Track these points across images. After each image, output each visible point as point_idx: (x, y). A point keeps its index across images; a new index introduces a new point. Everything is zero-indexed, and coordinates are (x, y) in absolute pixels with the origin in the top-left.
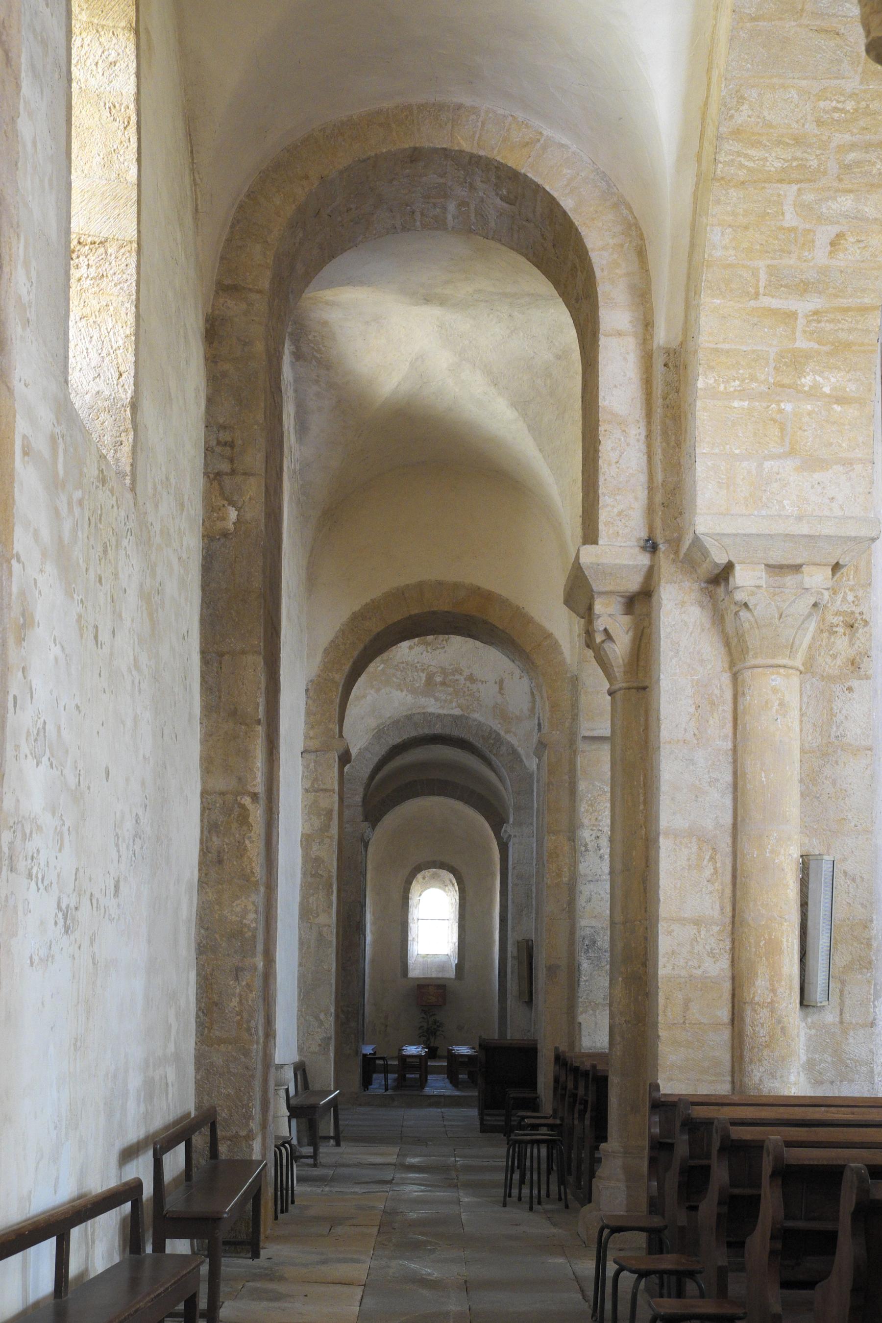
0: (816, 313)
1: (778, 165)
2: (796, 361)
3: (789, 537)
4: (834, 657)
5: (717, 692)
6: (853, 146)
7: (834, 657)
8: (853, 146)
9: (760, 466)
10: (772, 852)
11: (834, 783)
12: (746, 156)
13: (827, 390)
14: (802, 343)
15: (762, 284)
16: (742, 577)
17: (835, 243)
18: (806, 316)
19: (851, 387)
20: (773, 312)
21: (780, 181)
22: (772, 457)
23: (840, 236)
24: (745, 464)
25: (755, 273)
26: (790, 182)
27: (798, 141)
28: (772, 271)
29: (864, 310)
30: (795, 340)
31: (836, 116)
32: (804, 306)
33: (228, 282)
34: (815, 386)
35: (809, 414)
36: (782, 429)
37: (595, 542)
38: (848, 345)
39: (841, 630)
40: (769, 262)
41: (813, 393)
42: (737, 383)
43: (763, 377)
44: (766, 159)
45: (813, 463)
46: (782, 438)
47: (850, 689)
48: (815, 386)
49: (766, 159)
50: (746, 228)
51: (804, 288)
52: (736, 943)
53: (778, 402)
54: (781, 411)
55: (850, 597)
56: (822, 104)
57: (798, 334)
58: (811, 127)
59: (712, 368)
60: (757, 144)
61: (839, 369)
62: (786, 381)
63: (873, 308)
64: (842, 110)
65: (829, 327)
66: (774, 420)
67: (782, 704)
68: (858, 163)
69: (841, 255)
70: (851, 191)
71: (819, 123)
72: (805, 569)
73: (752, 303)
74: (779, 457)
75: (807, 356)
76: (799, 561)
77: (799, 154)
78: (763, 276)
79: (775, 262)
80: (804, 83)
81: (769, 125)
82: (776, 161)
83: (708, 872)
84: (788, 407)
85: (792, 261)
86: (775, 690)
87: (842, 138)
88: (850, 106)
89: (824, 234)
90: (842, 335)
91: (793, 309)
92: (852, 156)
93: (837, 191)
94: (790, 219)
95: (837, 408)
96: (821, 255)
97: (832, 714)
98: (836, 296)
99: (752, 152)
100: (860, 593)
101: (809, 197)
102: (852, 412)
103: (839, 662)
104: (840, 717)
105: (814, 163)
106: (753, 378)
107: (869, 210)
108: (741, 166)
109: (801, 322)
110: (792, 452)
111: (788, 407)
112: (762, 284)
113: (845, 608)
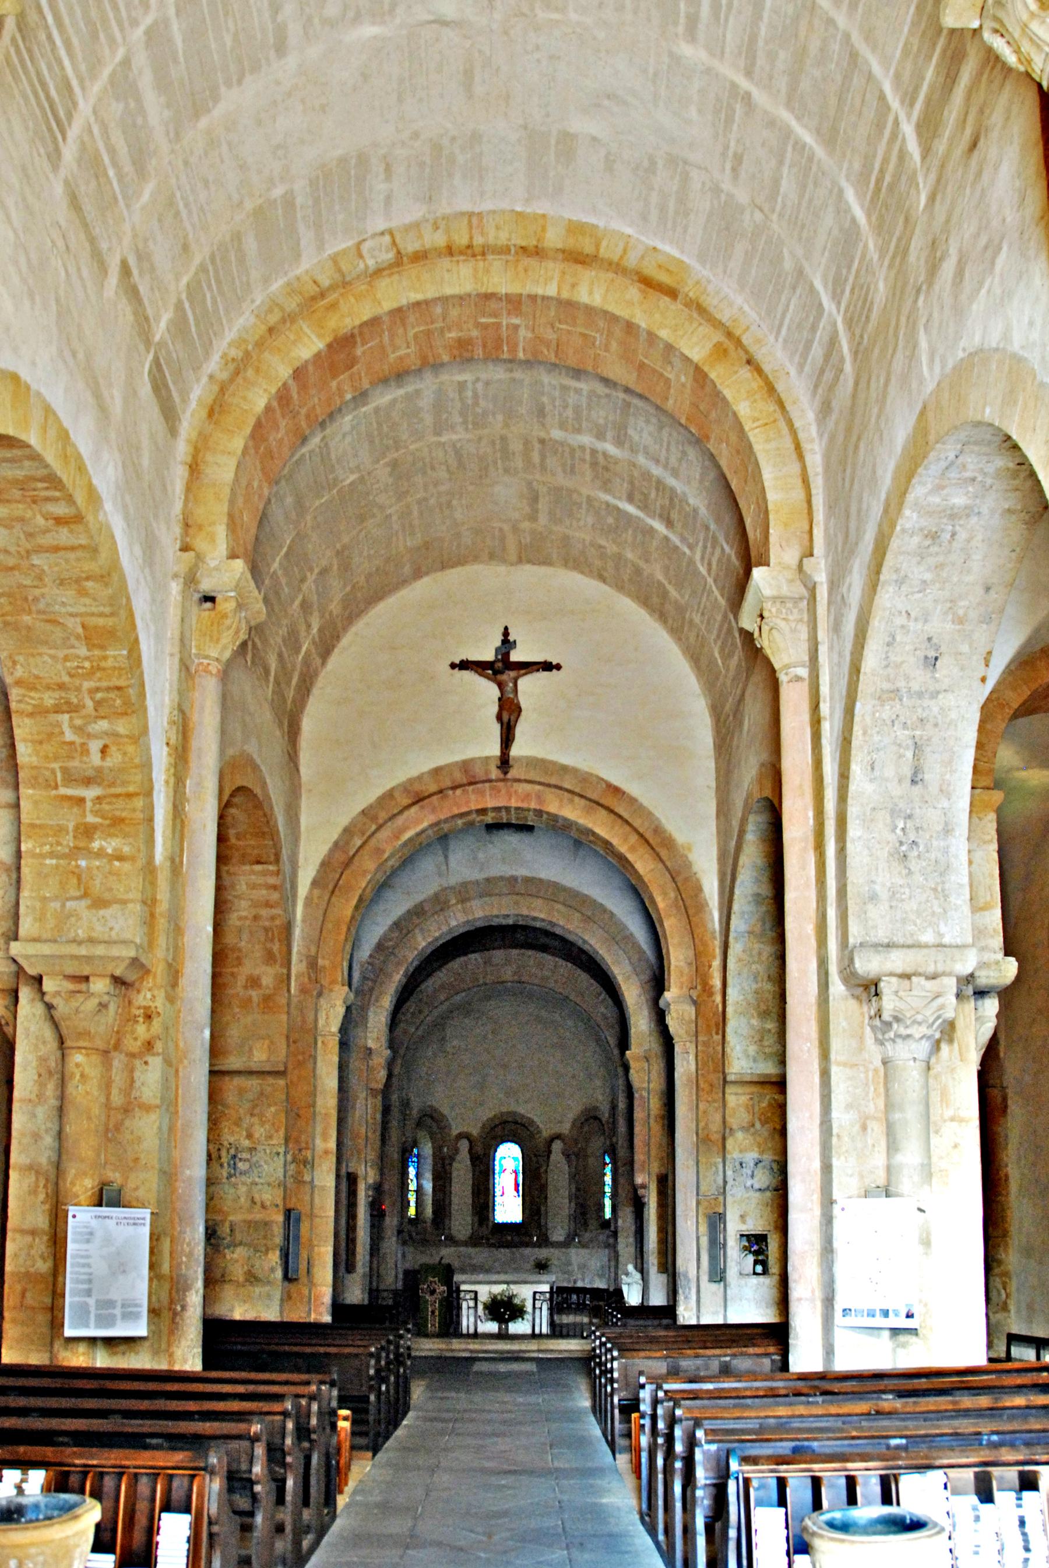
0: (98, 798)
1: (52, 702)
2: (87, 832)
4: (136, 1039)
7: (136, 1039)
9: (63, 906)
13: (109, 851)
16: (48, 985)
17: (104, 751)
19: (126, 849)
20: (69, 798)
21: (56, 712)
24: (52, 904)
25: (53, 772)
26: (63, 712)
27: (61, 686)
28: (65, 770)
29: (129, 796)
30: (85, 816)
32: (90, 793)
34: (102, 849)
36: (79, 879)
38: (122, 820)
39: (141, 1020)
41: (100, 854)
44: (42, 699)
45: (99, 903)
48: (102, 849)
51: (88, 782)
57: (88, 813)
58: (66, 679)
59: (30, 837)
60: (34, 688)
63: (137, 794)
65: (107, 807)
69: (108, 759)
70: (103, 718)
71: (71, 676)
72: (91, 979)
73: (54, 792)
74: (77, 898)
76: (86, 973)
81: (37, 677)
82: (49, 699)
85: (76, 763)
86: (77, 1065)
89: (95, 746)
90: (118, 813)
92: (99, 696)
95: (117, 863)
96: (96, 759)
98: (109, 786)
99: (32, 694)
101: (78, 722)
102: (127, 866)
105: (75, 701)
106: (58, 843)
107: (121, 730)
110: (85, 895)
113: (144, 1003)
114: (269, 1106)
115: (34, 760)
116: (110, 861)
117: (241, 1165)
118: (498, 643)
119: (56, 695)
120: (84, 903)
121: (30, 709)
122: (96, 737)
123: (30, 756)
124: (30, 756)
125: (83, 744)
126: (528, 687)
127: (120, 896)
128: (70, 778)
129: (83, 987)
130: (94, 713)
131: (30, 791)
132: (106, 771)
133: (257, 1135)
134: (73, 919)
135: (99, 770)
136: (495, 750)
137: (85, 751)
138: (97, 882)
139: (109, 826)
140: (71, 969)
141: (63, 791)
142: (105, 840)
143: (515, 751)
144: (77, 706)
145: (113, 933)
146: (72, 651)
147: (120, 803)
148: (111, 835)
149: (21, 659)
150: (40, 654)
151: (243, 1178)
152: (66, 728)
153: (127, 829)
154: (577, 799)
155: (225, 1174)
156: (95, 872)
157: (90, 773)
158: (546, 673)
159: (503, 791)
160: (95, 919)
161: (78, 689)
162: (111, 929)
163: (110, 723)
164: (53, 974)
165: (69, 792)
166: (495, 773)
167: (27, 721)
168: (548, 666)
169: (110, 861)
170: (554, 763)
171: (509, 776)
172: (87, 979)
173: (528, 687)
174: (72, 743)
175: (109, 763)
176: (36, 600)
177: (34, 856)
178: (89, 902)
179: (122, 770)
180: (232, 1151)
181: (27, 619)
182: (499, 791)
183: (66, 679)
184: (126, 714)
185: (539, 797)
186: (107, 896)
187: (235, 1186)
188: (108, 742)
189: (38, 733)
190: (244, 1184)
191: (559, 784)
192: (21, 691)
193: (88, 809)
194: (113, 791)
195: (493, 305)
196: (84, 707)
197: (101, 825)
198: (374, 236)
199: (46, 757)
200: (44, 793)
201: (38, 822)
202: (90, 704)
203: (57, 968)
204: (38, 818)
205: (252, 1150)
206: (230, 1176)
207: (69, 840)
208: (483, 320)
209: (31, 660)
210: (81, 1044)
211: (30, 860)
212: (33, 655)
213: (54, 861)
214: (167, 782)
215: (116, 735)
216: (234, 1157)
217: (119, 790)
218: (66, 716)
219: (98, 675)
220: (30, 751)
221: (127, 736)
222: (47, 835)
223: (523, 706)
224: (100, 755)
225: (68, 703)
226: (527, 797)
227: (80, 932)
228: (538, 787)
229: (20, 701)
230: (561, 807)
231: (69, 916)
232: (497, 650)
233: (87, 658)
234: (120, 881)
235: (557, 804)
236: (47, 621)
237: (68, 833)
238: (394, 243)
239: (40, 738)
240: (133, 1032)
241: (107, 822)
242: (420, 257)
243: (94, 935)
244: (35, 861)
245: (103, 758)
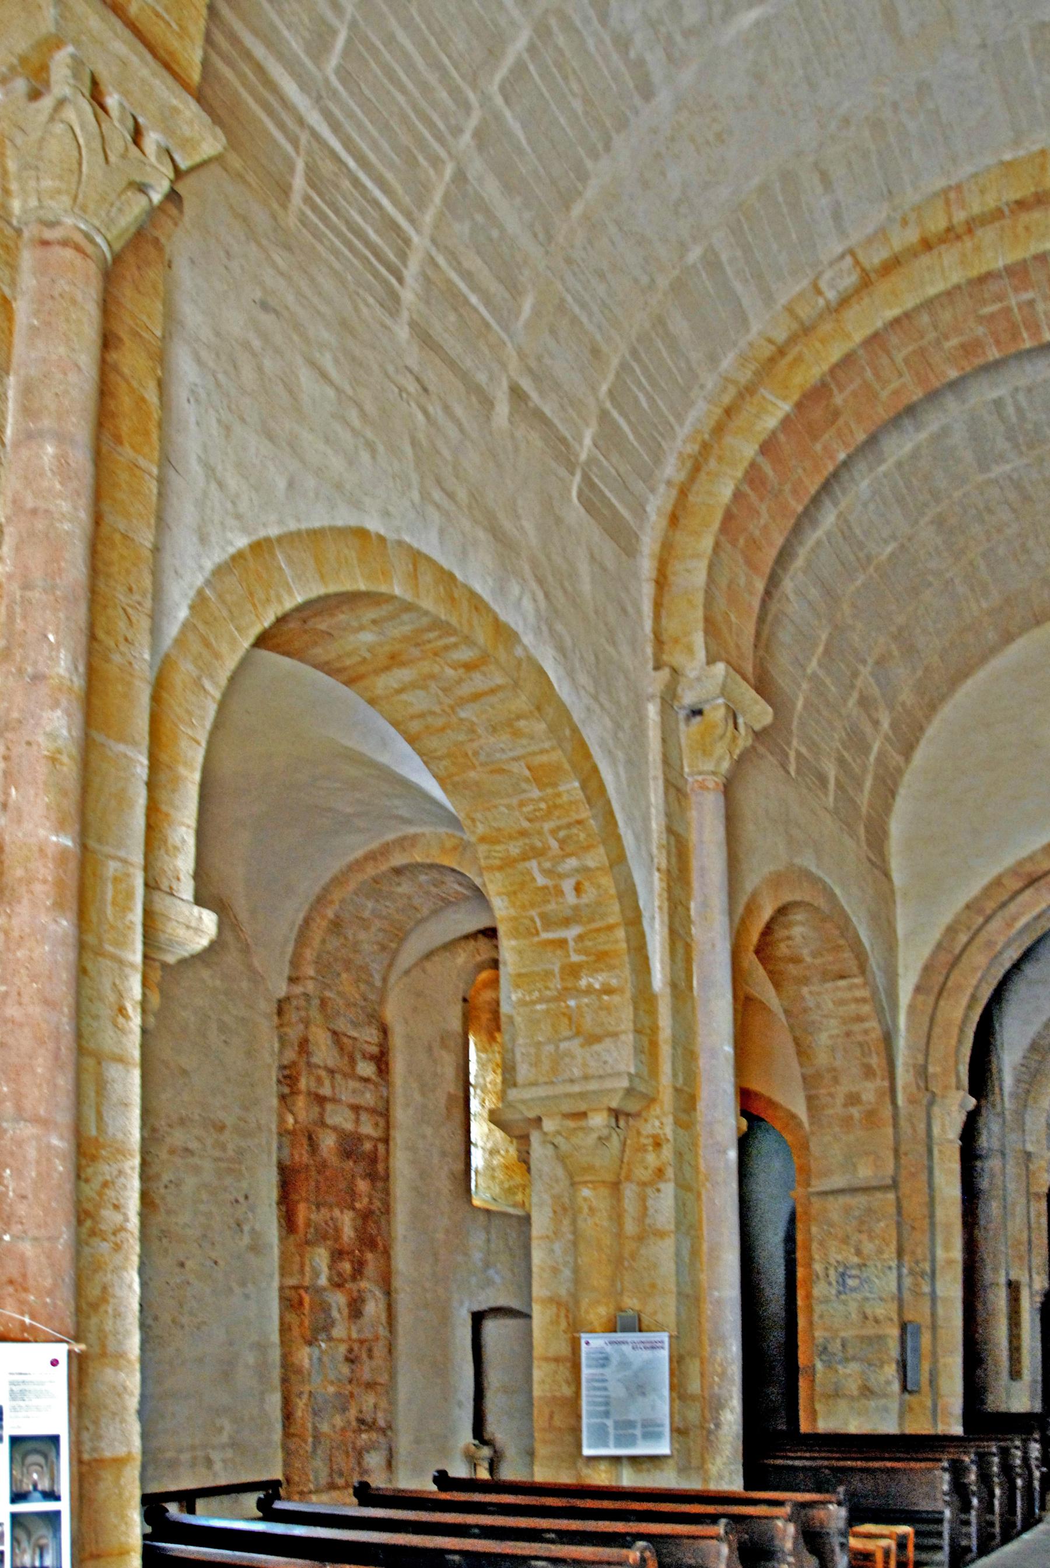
3: (568, 1095)
8: (559, 828)
13: (597, 986)
14: (575, 958)
17: (578, 889)
19: (614, 982)
27: (523, 833)
29: (610, 928)
34: (590, 986)
38: (606, 953)
40: (539, 910)
41: (589, 991)
45: (593, 1039)
46: (570, 1026)
48: (590, 986)
56: (525, 809)
58: (526, 824)
61: (602, 970)
62: (569, 985)
64: (540, 809)
65: (590, 944)
68: (569, 837)
71: (530, 820)
72: (590, 1114)
81: (499, 830)
82: (514, 849)
87: (547, 826)
88: (543, 805)
89: (568, 886)
90: (601, 948)
94: (541, 881)
95: (606, 998)
96: (571, 898)
101: (547, 865)
102: (616, 999)
105: (539, 844)
109: (571, 943)
114: (879, 1220)
116: (599, 999)
117: (850, 1282)
119: (520, 843)
120: (577, 1042)
122: (567, 876)
129: (583, 1123)
133: (865, 1251)
135: (576, 908)
137: (559, 892)
140: (567, 1107)
146: (524, 796)
147: (602, 938)
148: (596, 971)
151: (854, 1295)
155: (834, 1292)
157: (569, 913)
161: (540, 833)
175: (585, 899)
176: (476, 754)
179: (599, 904)
180: (841, 1270)
181: (472, 774)
183: (526, 824)
186: (598, 1031)
187: (845, 1303)
188: (579, 877)
190: (854, 1300)
195: (993, 287)
196: (549, 848)
198: (831, 264)
202: (554, 844)
205: (862, 1266)
206: (839, 1293)
208: (987, 310)
210: (588, 1178)
212: (489, 809)
214: (660, 908)
216: (843, 1275)
224: (574, 893)
225: (533, 848)
233: (542, 799)
236: (492, 772)
238: (857, 262)
242: (891, 265)
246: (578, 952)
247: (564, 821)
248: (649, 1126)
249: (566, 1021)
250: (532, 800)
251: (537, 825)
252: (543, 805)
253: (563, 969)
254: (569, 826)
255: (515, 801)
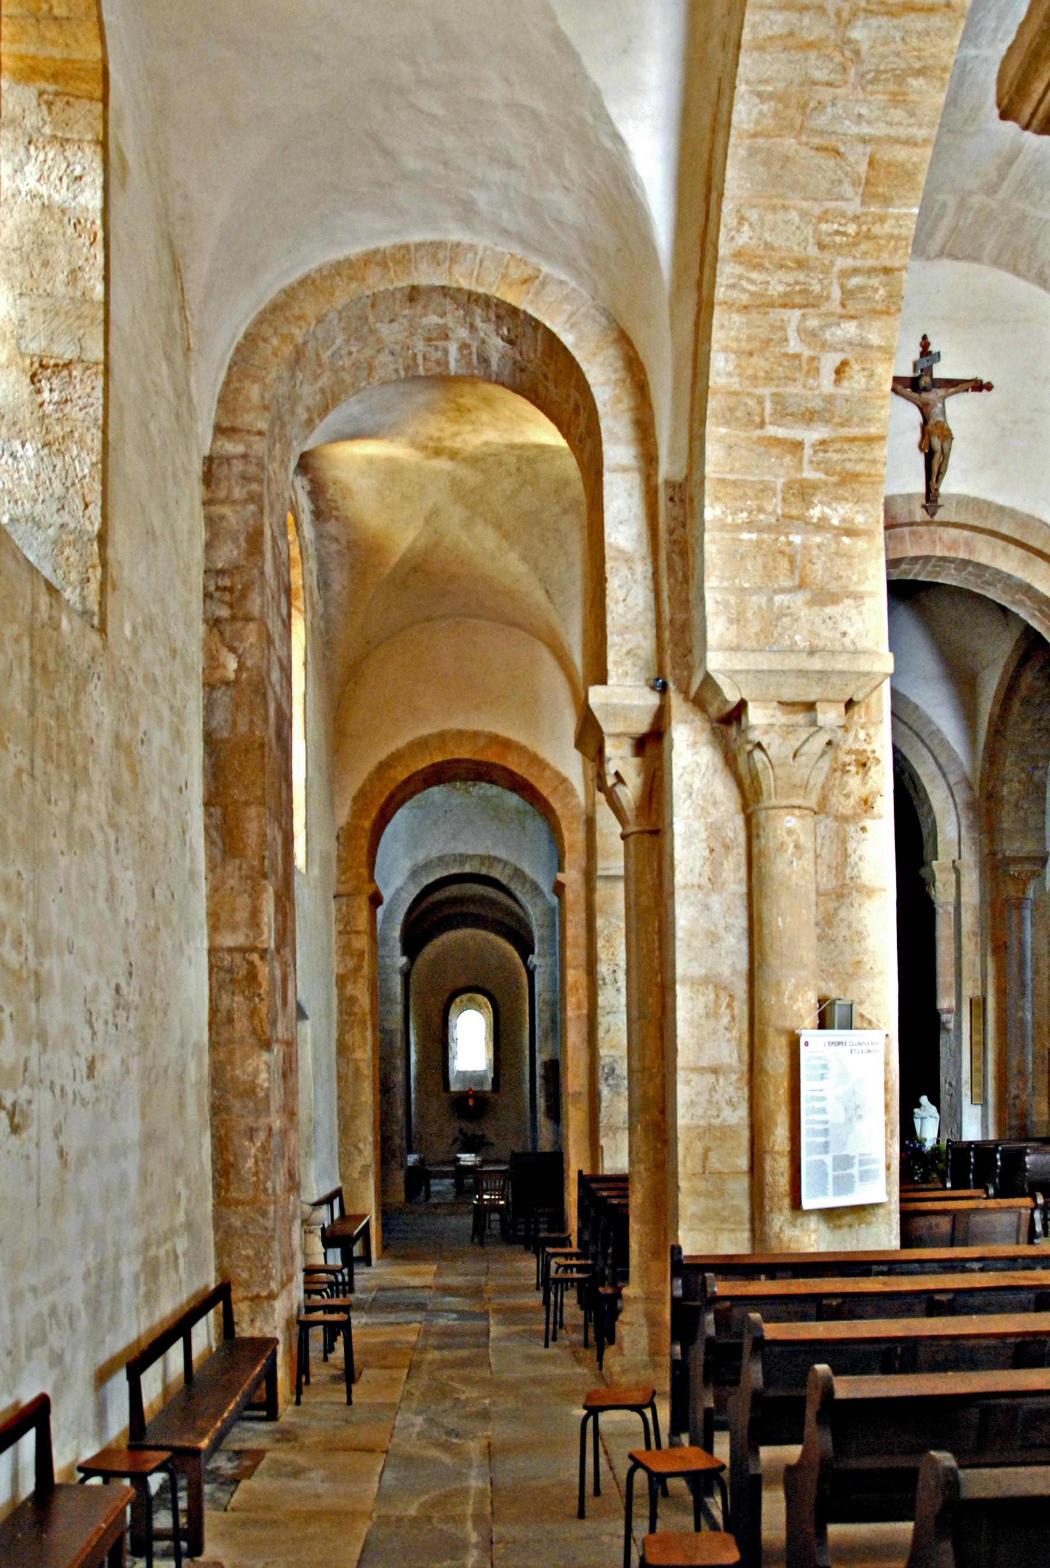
0: (823, 442)
1: (781, 288)
3: (802, 673)
5: (731, 834)
6: (855, 271)
7: (847, 796)
8: (855, 271)
9: (770, 600)
10: (790, 998)
11: (849, 926)
12: (748, 279)
13: (835, 521)
14: (809, 474)
15: (768, 411)
16: (756, 716)
17: (840, 371)
18: (814, 446)
19: (860, 519)
20: (778, 442)
21: (784, 306)
22: (783, 591)
23: (844, 363)
24: (755, 598)
26: (794, 307)
27: (801, 264)
28: (778, 400)
30: (801, 470)
31: (838, 239)
32: (811, 435)
33: (226, 424)
34: (824, 519)
35: (819, 546)
36: (792, 561)
37: (603, 681)
38: (855, 476)
39: (853, 769)
41: (822, 525)
42: (745, 514)
43: (770, 509)
44: (768, 283)
46: (792, 572)
47: (863, 829)
48: (824, 519)
49: (768, 283)
50: (751, 354)
51: (809, 417)
52: (755, 1091)
53: (787, 534)
54: (790, 543)
55: (862, 735)
56: (824, 227)
58: (813, 251)
59: (717, 499)
60: (759, 267)
61: (846, 500)
62: (794, 512)
64: (844, 234)
65: (835, 457)
66: (782, 553)
67: (797, 846)
68: (862, 289)
69: (846, 383)
70: (853, 317)
71: (821, 246)
72: (818, 706)
73: (758, 433)
75: (815, 486)
76: (812, 698)
77: (801, 278)
78: (768, 405)
79: (780, 390)
80: (805, 204)
81: (769, 247)
82: (777, 285)
83: (725, 1020)
84: (797, 539)
86: (790, 832)
87: (844, 262)
89: (830, 362)
90: (849, 466)
91: (799, 438)
93: (842, 317)
94: (794, 345)
95: (846, 540)
96: (826, 382)
97: (846, 856)
98: (842, 425)
99: (754, 275)
100: (872, 731)
101: (813, 323)
102: (861, 544)
103: (852, 801)
104: (854, 858)
105: (817, 288)
106: (761, 510)
107: (874, 339)
108: (744, 290)
109: (808, 451)
110: (802, 586)
111: (797, 539)
112: (768, 411)
113: (857, 746)
115: (735, 383)
116: (837, 537)
118: (916, 356)
119: (790, 278)
121: (745, 298)
122: (834, 348)
123: (730, 375)
124: (730, 375)
125: (813, 359)
126: (958, 410)
127: (852, 588)
128: (783, 412)
130: (839, 310)
131: (723, 430)
132: (840, 402)
134: (786, 621)
135: (830, 399)
136: (919, 487)
137: (814, 371)
138: (819, 566)
139: (835, 484)
141: (772, 431)
142: (829, 505)
143: (950, 486)
144: (819, 297)
145: (847, 641)
147: (854, 452)
148: (838, 499)
149: (753, 215)
150: (785, 208)
152: (792, 334)
153: (863, 491)
154: (1012, 548)
156: (815, 552)
157: (817, 404)
158: (976, 394)
159: (926, 537)
160: (818, 621)
161: (826, 270)
162: (844, 634)
163: (860, 326)
164: (764, 701)
165: (781, 432)
166: (920, 515)
167: (736, 317)
168: (979, 386)
169: (837, 537)
170: (988, 504)
171: (937, 518)
172: (810, 707)
173: (958, 410)
174: (797, 356)
175: (845, 389)
177: (723, 527)
178: (808, 596)
179: (863, 401)
182: (921, 537)
184: (888, 313)
185: (968, 544)
186: (834, 587)
188: (849, 356)
189: (750, 339)
191: (995, 528)
192: (739, 270)
193: (806, 459)
194: (845, 432)
196: (828, 298)
197: (826, 484)
199: (754, 378)
200: (743, 435)
201: (731, 477)
202: (836, 293)
203: (772, 691)
204: (731, 471)
207: (775, 505)
209: (769, 217)
211: (718, 535)
213: (754, 536)
215: (864, 345)
217: (855, 431)
218: (797, 313)
219: (863, 247)
220: (730, 368)
221: (880, 348)
222: (744, 497)
223: (955, 432)
224: (833, 376)
225: (805, 292)
226: (954, 545)
227: (797, 638)
228: (966, 533)
229: (732, 287)
230: (994, 557)
231: (780, 616)
232: (915, 365)
234: (850, 564)
235: (989, 553)
237: (775, 494)
239: (748, 347)
240: (843, 785)
241: (835, 479)
243: (820, 643)
244: (727, 536)
245: (837, 381)
246: (817, 465)
247: (870, 262)
248: (852, 734)
249: (786, 565)
250: (843, 215)
251: (827, 257)
252: (852, 229)
253: (788, 486)
254: (871, 271)
255: (817, 209)
